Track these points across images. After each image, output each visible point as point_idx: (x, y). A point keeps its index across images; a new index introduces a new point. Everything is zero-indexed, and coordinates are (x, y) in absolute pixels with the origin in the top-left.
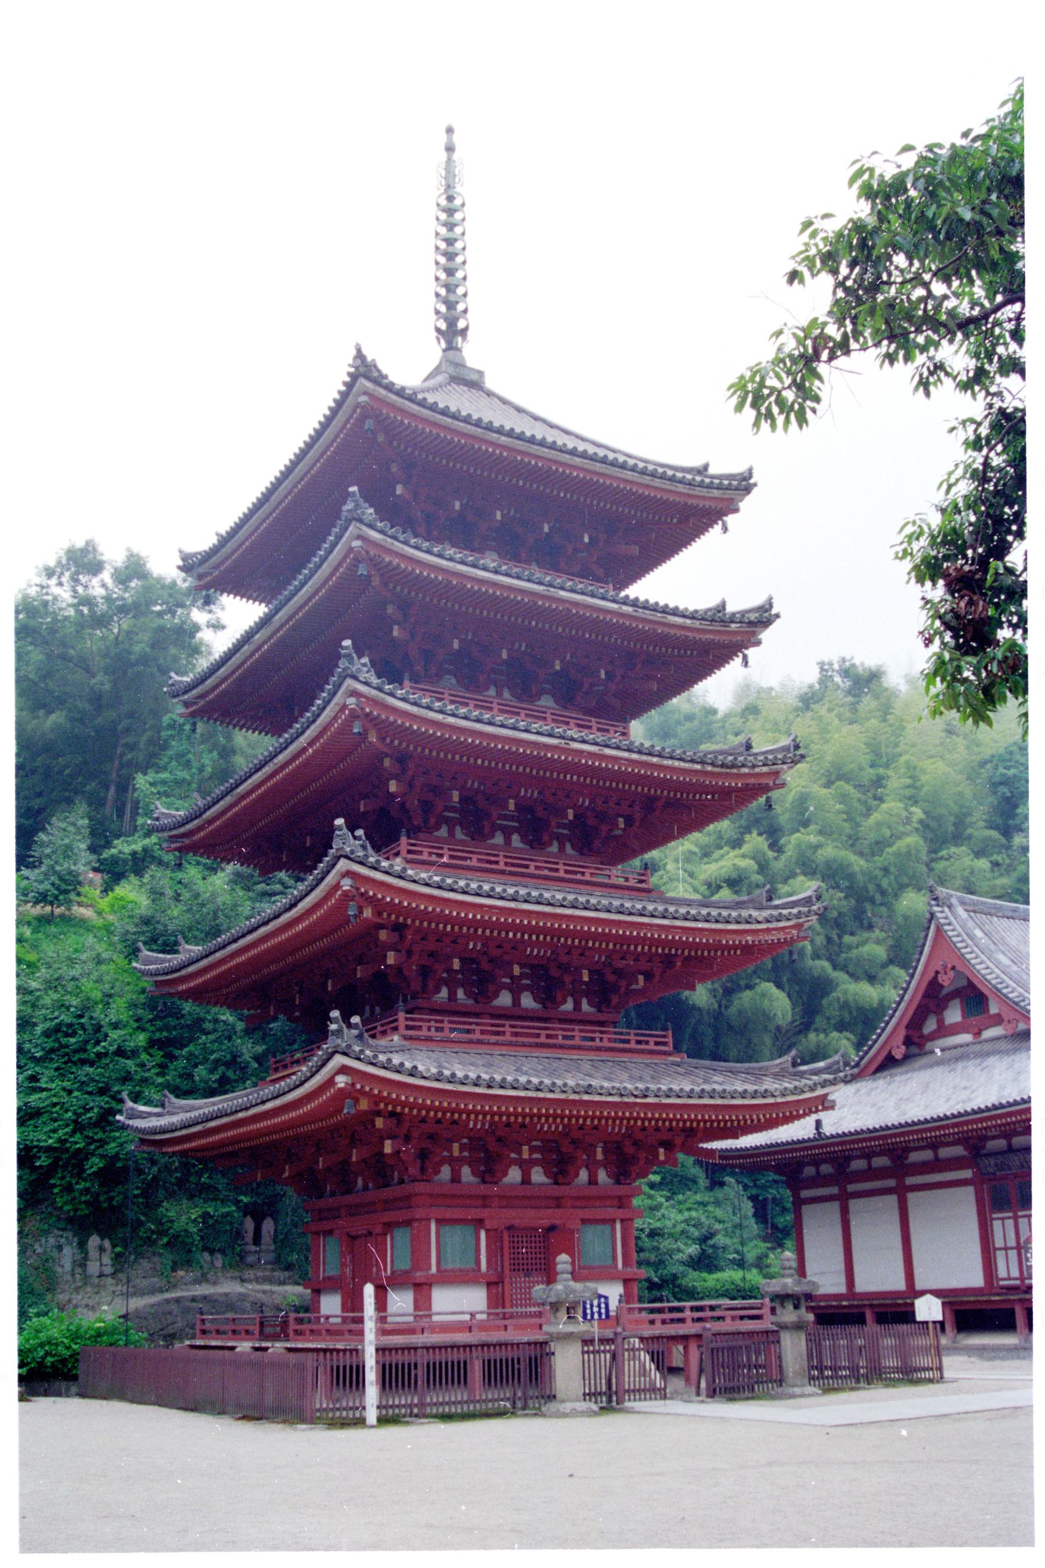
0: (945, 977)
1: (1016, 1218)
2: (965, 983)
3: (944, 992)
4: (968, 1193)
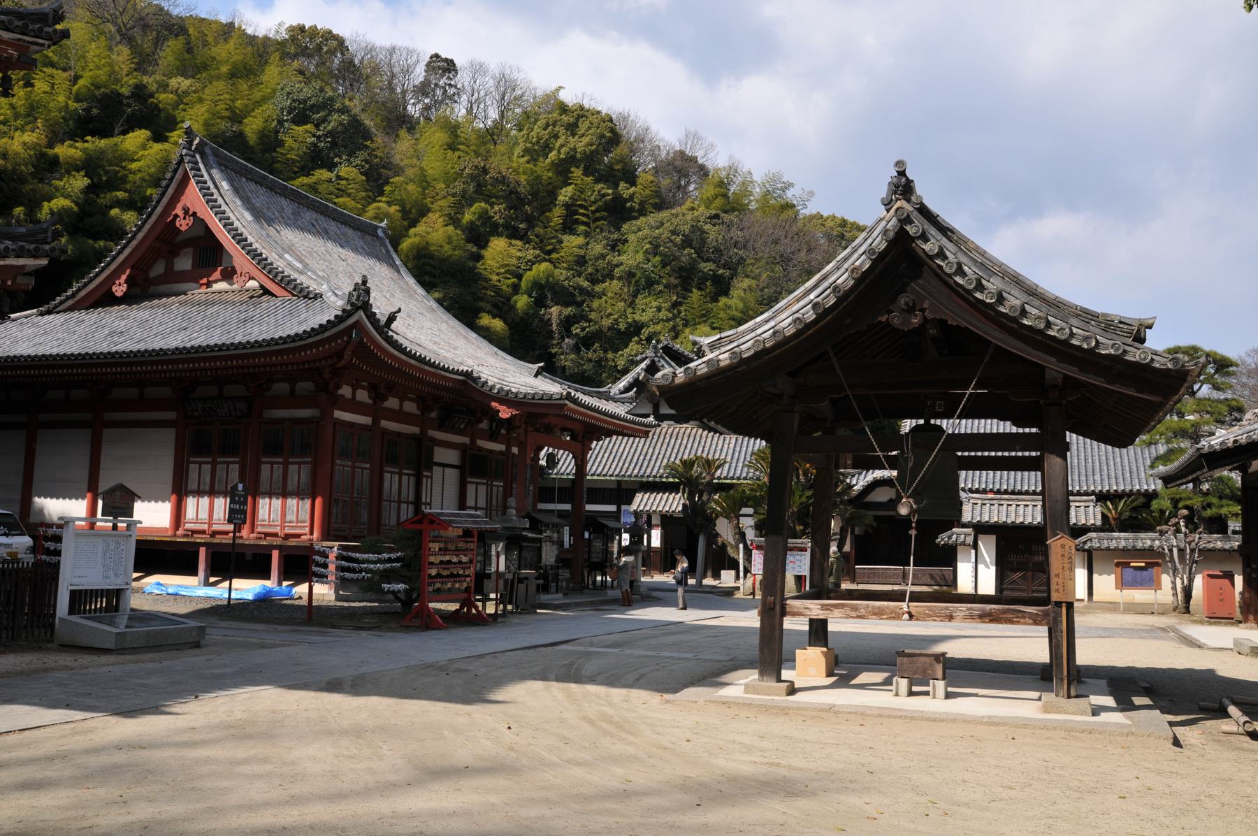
0: (183, 222)
1: (214, 465)
2: (202, 232)
3: (180, 238)
4: (169, 435)
